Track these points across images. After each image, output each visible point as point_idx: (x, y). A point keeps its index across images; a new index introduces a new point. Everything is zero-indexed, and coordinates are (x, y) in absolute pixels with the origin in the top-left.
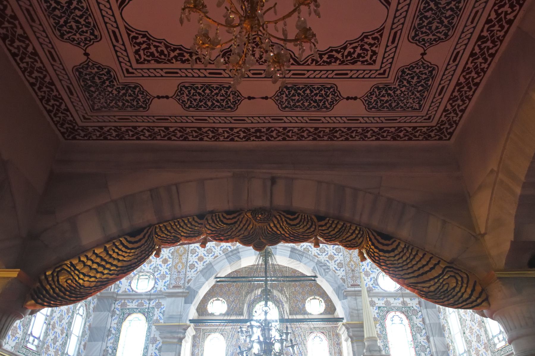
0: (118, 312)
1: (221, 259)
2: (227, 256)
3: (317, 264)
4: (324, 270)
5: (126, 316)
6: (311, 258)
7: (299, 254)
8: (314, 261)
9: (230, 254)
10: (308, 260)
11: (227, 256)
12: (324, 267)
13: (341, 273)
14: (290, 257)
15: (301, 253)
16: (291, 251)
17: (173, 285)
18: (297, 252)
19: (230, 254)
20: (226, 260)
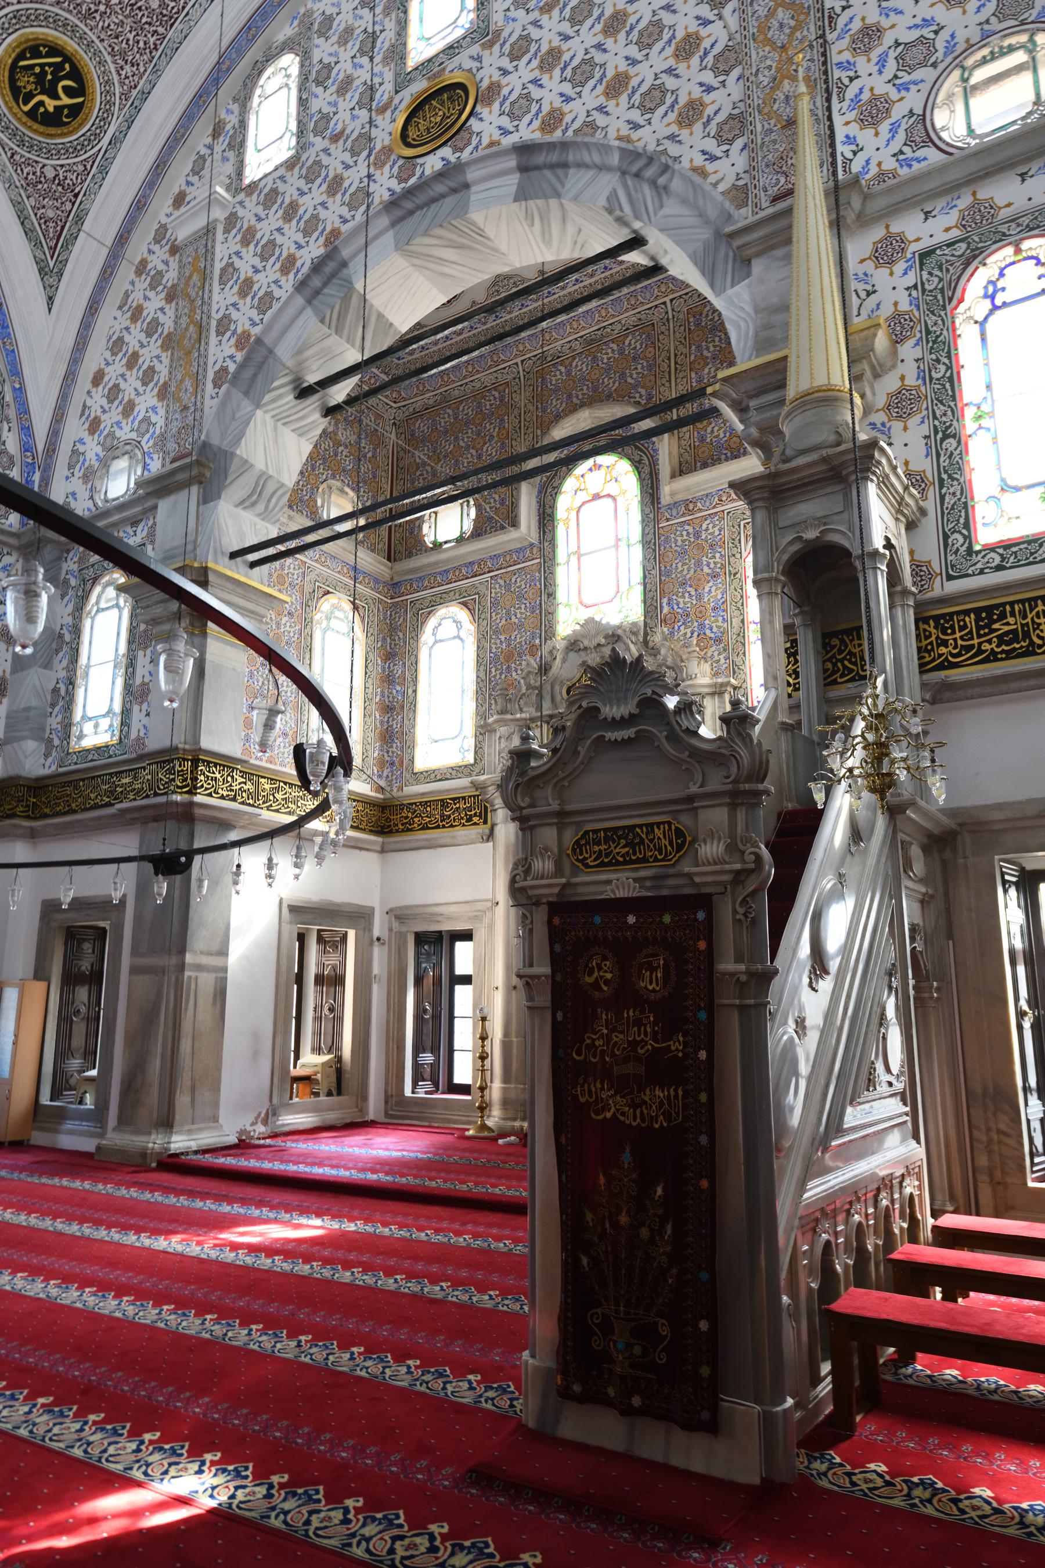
0: (73, 582)
1: (290, 311)
2: (308, 292)
3: (624, 173)
4: (653, 183)
5: (88, 586)
6: (596, 158)
7: (552, 167)
8: (609, 169)
9: (316, 282)
10: (591, 173)
11: (308, 292)
12: (649, 173)
13: (731, 166)
14: (522, 195)
15: (554, 157)
16: (523, 169)
17: (172, 455)
18: (540, 159)
19: (316, 282)
20: (309, 311)
